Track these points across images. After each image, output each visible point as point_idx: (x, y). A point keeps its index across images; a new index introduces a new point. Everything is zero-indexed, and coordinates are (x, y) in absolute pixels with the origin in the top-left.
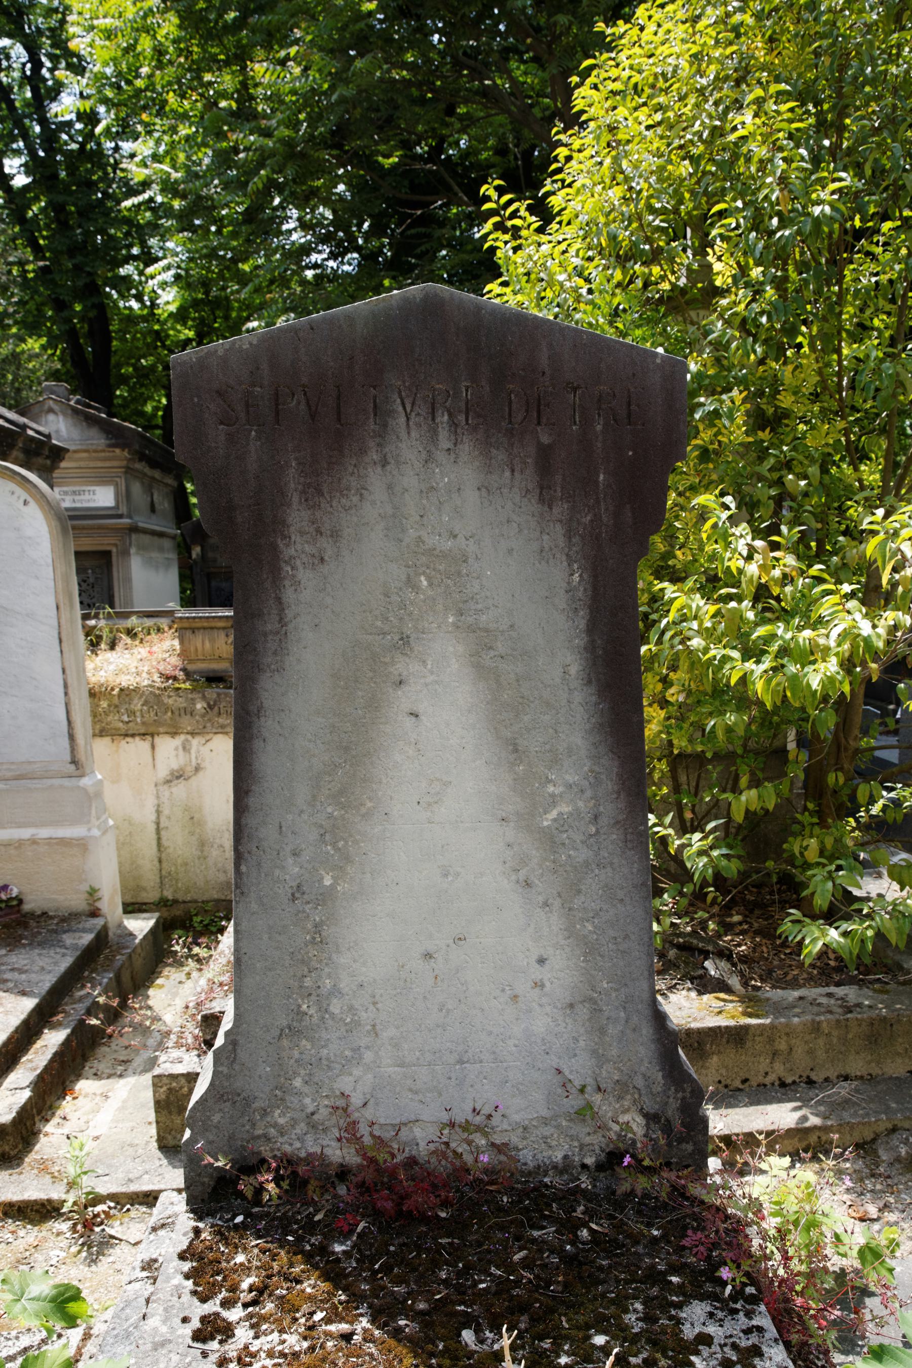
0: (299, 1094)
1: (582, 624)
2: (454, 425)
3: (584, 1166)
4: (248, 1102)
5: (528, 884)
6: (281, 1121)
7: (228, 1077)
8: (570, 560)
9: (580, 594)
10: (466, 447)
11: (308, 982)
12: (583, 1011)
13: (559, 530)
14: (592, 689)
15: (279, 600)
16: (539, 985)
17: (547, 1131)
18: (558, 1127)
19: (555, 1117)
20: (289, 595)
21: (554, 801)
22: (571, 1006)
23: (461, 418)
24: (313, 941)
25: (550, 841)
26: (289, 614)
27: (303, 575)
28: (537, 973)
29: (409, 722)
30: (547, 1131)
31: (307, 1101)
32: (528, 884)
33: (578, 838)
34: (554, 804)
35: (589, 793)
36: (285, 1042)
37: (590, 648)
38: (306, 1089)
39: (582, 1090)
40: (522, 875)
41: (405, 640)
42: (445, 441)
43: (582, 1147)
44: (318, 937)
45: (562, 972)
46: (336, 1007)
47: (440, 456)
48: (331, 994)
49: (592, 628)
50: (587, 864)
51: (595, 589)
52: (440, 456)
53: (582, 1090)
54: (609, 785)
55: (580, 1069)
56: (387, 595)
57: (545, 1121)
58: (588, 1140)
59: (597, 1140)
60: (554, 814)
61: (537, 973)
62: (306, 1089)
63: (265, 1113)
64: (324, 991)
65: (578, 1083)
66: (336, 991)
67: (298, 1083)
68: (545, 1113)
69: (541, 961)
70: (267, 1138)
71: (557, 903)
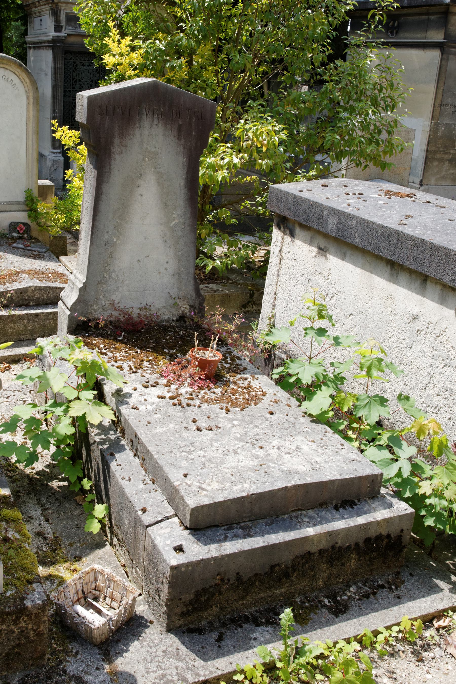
0: (101, 300)
1: (185, 172)
2: (158, 118)
3: (173, 320)
4: (87, 303)
5: (166, 241)
6: (96, 308)
7: (83, 295)
8: (184, 155)
9: (185, 164)
10: (161, 124)
11: (107, 268)
12: (177, 276)
13: (182, 147)
14: (186, 189)
15: (110, 163)
16: (166, 269)
17: (164, 310)
18: (167, 309)
19: (167, 306)
20: (112, 162)
21: (174, 219)
22: (174, 275)
23: (160, 116)
24: (109, 257)
25: (172, 230)
26: (112, 167)
27: (117, 157)
28: (166, 266)
29: (140, 197)
30: (164, 310)
31: (103, 302)
32: (166, 241)
33: (179, 229)
34: (174, 220)
35: (183, 217)
36: (99, 285)
37: (187, 178)
38: (103, 299)
39: (174, 299)
40: (164, 239)
41: (141, 175)
42: (155, 123)
43: (173, 315)
44: (111, 256)
45: (172, 266)
46: (113, 275)
47: (154, 126)
48: (112, 271)
49: (188, 173)
50: (181, 236)
51: (189, 163)
52: (154, 126)
53: (174, 299)
54: (188, 215)
55: (174, 292)
56: (137, 163)
57: (164, 307)
58: (174, 313)
59: (176, 313)
60: (174, 223)
61: (166, 266)
62: (103, 299)
63: (91, 306)
64: (111, 271)
65: (173, 297)
66: (114, 271)
67: (101, 297)
68: (164, 305)
69: (167, 262)
70: (91, 313)
71: (172, 247)
